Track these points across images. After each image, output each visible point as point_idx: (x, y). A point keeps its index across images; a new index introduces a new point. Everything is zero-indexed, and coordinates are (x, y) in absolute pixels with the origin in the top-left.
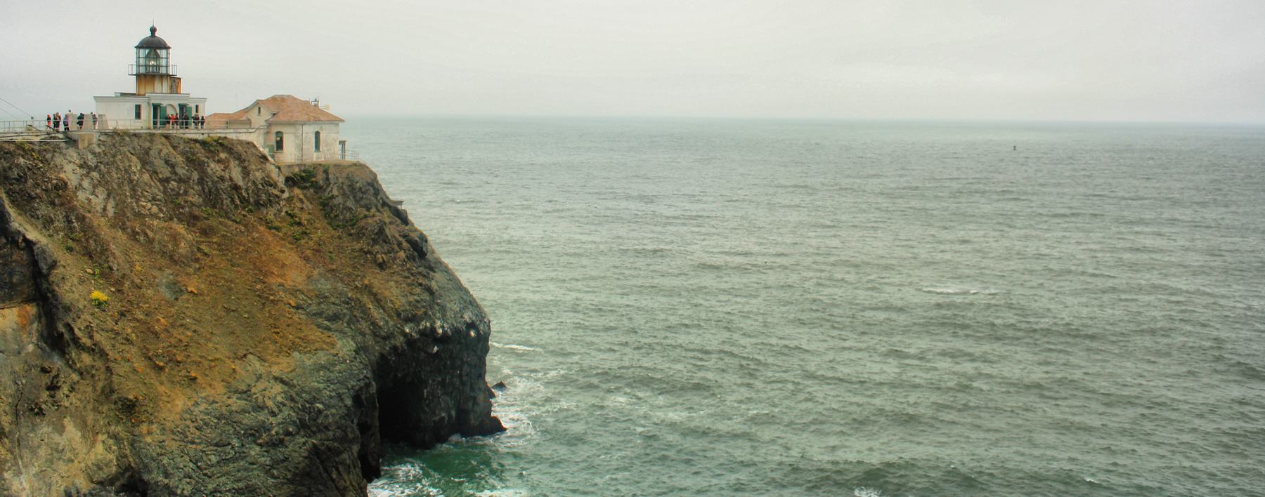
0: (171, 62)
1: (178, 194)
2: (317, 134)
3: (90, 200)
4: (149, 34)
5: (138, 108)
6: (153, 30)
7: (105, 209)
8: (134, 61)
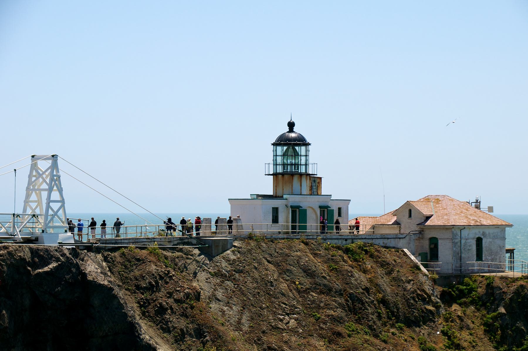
0: (311, 160)
1: (319, 307)
2: (479, 241)
3: (223, 312)
4: (287, 129)
5: (275, 211)
6: (291, 125)
7: (239, 322)
8: (270, 159)
